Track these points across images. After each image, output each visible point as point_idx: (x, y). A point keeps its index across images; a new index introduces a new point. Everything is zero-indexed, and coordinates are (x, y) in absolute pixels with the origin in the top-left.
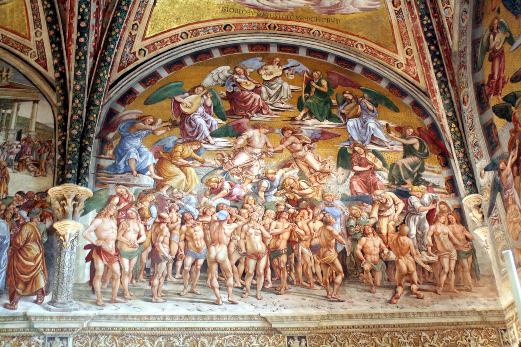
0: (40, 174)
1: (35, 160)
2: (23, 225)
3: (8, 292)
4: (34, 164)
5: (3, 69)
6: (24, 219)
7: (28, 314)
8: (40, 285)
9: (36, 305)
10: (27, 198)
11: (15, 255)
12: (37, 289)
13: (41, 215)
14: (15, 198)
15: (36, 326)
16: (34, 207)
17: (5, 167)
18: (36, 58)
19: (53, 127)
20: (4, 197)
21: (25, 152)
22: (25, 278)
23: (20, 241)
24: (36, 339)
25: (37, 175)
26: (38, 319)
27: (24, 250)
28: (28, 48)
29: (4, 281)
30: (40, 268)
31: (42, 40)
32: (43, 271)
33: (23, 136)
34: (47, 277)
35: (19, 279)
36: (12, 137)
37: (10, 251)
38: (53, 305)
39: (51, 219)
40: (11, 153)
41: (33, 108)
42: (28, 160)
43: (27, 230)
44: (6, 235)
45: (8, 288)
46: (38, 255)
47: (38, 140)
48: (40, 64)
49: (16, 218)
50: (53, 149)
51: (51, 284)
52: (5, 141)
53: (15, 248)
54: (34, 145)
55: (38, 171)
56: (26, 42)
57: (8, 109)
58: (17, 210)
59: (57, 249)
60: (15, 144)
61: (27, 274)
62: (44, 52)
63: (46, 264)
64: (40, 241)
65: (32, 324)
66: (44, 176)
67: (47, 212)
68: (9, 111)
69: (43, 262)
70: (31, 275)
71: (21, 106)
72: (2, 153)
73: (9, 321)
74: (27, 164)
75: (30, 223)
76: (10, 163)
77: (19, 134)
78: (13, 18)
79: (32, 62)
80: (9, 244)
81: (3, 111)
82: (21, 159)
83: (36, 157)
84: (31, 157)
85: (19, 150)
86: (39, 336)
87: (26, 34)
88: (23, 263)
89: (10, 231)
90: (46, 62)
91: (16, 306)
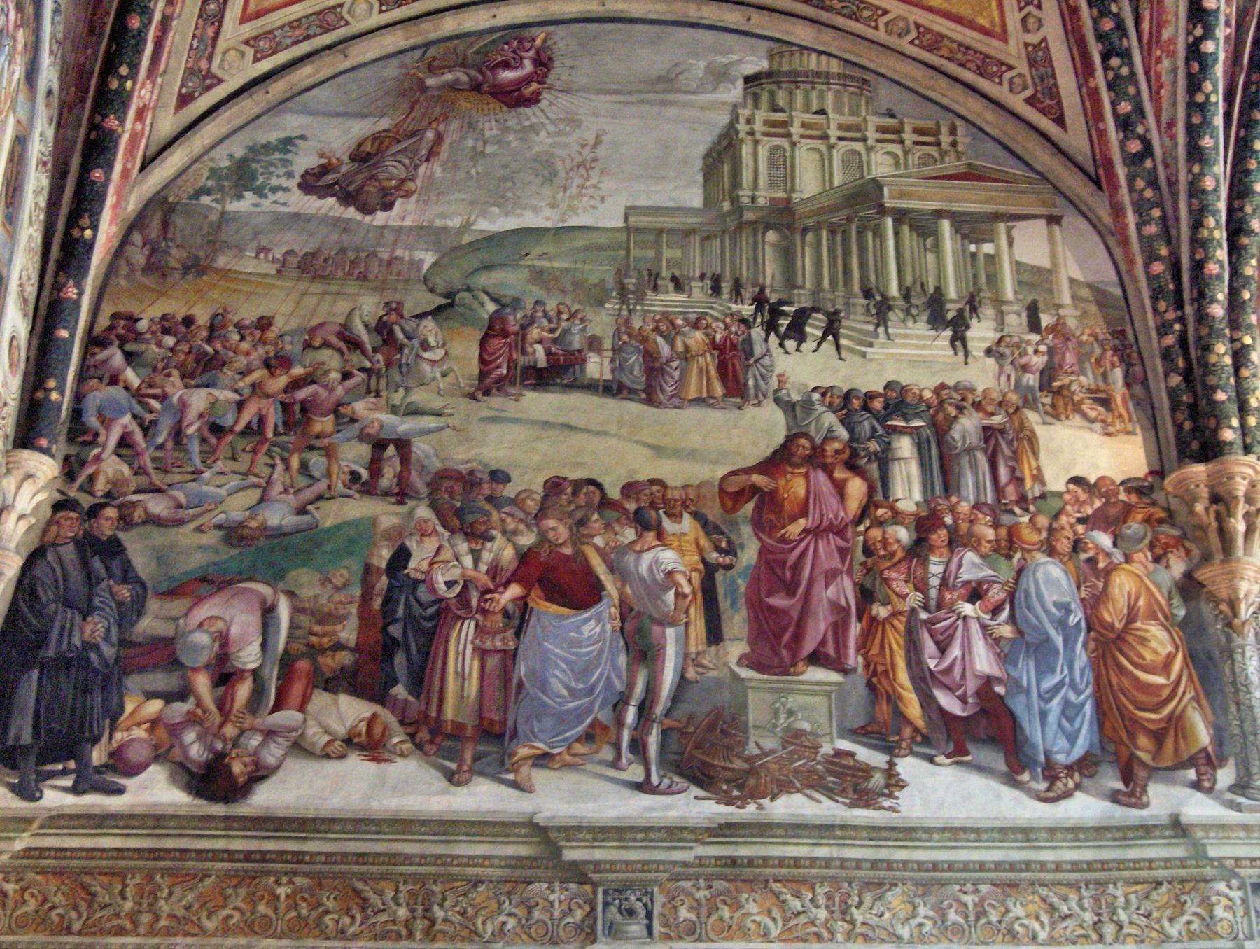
0: (1118, 426)
1: (1093, 387)
2: (1107, 573)
3: (1113, 758)
4: (1095, 400)
5: (938, 125)
6: (1108, 555)
7: (1184, 820)
8: (1196, 740)
9: (1199, 795)
10: (1101, 496)
11: (1108, 655)
12: (1193, 751)
13: (1151, 542)
14: (1067, 497)
15: (1213, 852)
16: (1125, 522)
17: (1017, 409)
19: (1118, 292)
20: (1037, 494)
21: (1061, 366)
22: (1149, 720)
23: (1113, 615)
24: (1222, 886)
25: (1111, 429)
26: (1212, 834)
27: (1130, 644)
28: (1002, 63)
29: (1095, 727)
30: (1187, 692)
31: (1044, 40)
32: (1196, 699)
33: (1046, 320)
34: (1211, 718)
35: (1136, 722)
36: (1016, 321)
37: (1092, 645)
38: (1243, 795)
39: (1183, 554)
40: (1025, 368)
41: (1051, 239)
42: (1074, 387)
43: (1123, 586)
44: (1068, 599)
45: (1111, 747)
46: (1170, 658)
47: (1087, 331)
49: (1085, 551)
50: (1135, 355)
51: (1226, 735)
52: (999, 335)
53: (1102, 635)
54: (1081, 344)
55: (1110, 420)
56: (992, 47)
57: (984, 241)
58: (1080, 529)
59: (1219, 639)
60: (1028, 342)
61: (1154, 710)
63: (1201, 679)
64: (1166, 617)
65: (1200, 848)
66: (1128, 433)
67: (1167, 535)
68: (988, 248)
69: (1190, 675)
70: (1166, 711)
71: (1015, 233)
72: (1001, 367)
73: (1134, 838)
74: (1076, 398)
75: (1125, 566)
76: (1030, 397)
77: (1033, 312)
79: (1017, 102)
80: (1083, 624)
81: (973, 248)
82: (1056, 384)
83: (1095, 378)
84: (1082, 378)
85: (1045, 358)
86: (1228, 881)
87: (992, 23)
88: (1136, 679)
89: (1078, 588)
91: (1145, 799)
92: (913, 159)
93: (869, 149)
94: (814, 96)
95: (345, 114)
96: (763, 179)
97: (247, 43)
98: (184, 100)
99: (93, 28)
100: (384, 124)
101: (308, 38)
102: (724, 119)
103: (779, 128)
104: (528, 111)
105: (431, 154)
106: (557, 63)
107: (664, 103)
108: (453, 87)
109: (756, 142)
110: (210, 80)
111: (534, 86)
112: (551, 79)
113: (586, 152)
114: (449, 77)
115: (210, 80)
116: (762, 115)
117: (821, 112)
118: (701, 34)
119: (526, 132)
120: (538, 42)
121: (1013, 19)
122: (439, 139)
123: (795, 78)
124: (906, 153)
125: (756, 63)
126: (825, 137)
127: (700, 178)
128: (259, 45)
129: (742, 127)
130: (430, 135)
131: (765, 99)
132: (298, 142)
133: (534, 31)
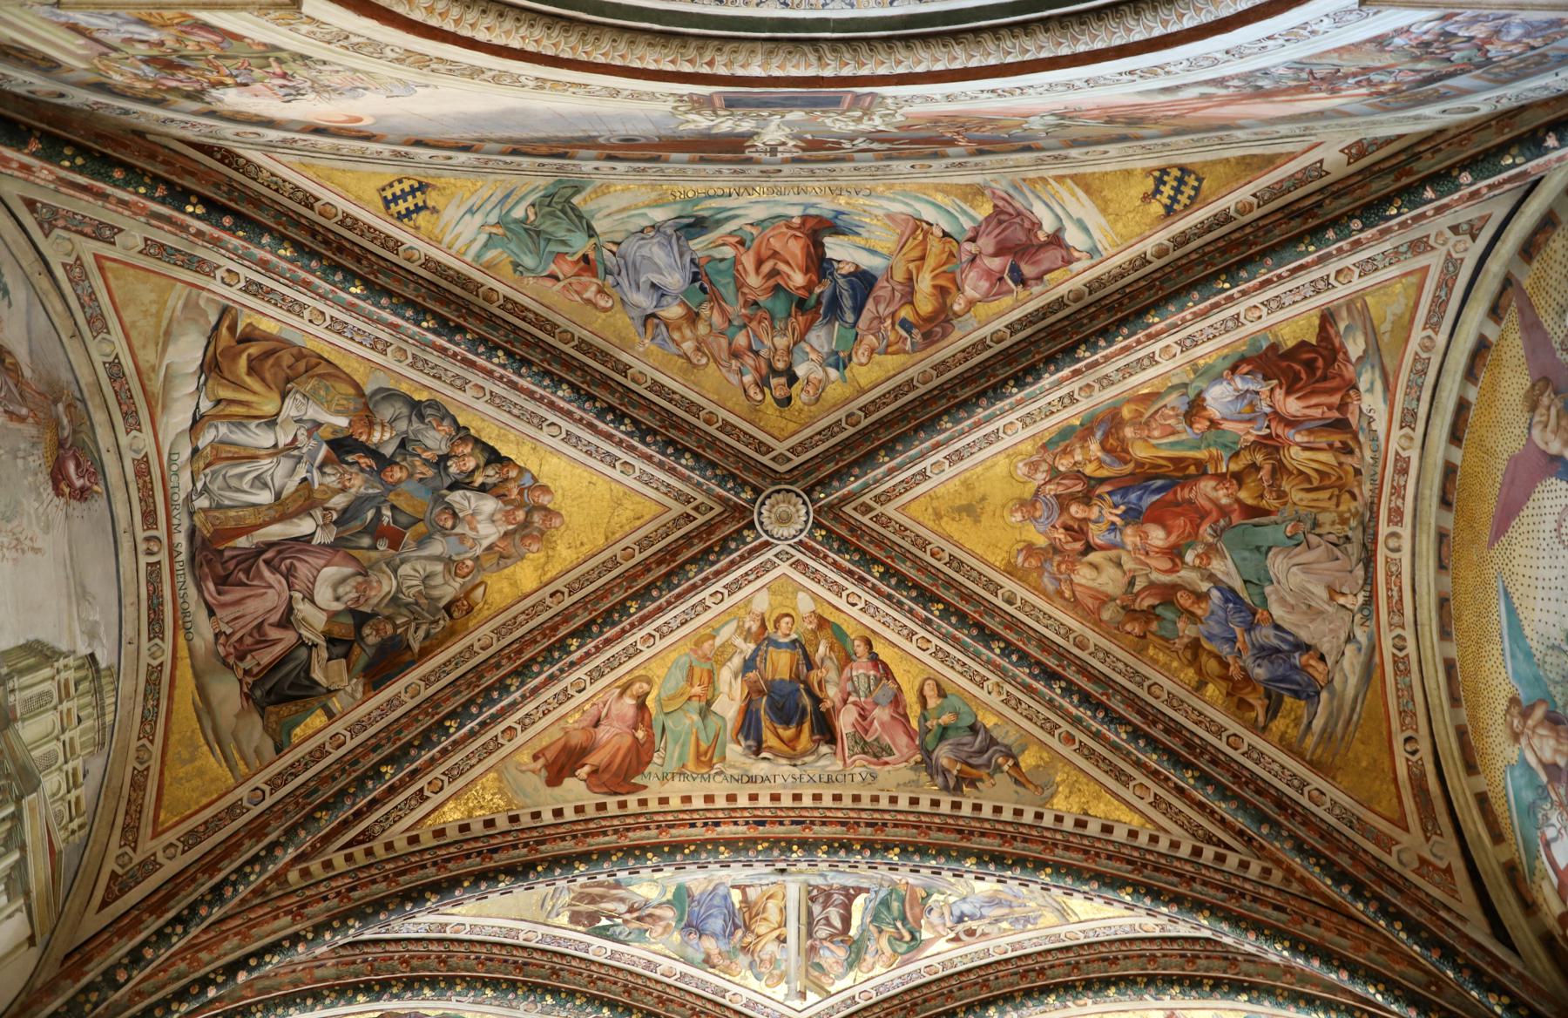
18: (120, 871)
28: (136, 842)
48: (108, 887)
56: (146, 830)
62: (138, 883)
78: (188, 781)
79: (110, 865)
90: (117, 898)
92: (59, 806)
93: (60, 769)
94: (89, 710)
95: (30, 340)
96: (27, 693)
97: (78, 258)
98: (31, 204)
99: (100, 137)
100: (28, 373)
101: (83, 306)
102: (64, 646)
103: (64, 694)
104: (50, 489)
105: (11, 415)
106: (84, 505)
107: (69, 596)
108: (58, 424)
109: (53, 678)
110: (47, 226)
111: (67, 490)
112: (73, 503)
113: (28, 542)
114: (65, 421)
115: (47, 226)
116: (71, 675)
117: (80, 720)
118: (115, 609)
119: (35, 489)
120: (96, 488)
121: (170, 837)
122: (22, 419)
123: (98, 691)
124: (62, 798)
125: (104, 660)
126: (63, 731)
127: (22, 641)
128: (76, 268)
129: (62, 662)
130: (24, 411)
131: (82, 673)
132: (6, 302)
133: (102, 482)
